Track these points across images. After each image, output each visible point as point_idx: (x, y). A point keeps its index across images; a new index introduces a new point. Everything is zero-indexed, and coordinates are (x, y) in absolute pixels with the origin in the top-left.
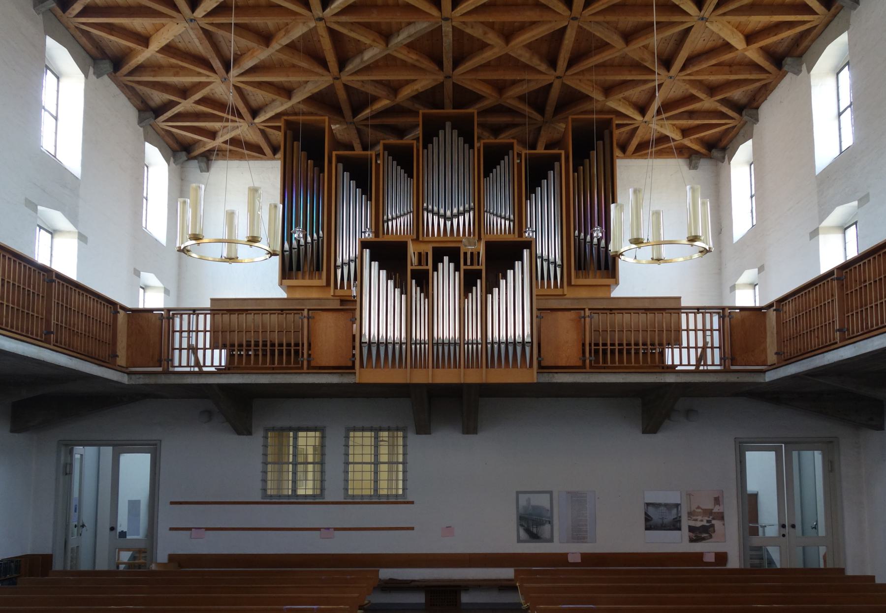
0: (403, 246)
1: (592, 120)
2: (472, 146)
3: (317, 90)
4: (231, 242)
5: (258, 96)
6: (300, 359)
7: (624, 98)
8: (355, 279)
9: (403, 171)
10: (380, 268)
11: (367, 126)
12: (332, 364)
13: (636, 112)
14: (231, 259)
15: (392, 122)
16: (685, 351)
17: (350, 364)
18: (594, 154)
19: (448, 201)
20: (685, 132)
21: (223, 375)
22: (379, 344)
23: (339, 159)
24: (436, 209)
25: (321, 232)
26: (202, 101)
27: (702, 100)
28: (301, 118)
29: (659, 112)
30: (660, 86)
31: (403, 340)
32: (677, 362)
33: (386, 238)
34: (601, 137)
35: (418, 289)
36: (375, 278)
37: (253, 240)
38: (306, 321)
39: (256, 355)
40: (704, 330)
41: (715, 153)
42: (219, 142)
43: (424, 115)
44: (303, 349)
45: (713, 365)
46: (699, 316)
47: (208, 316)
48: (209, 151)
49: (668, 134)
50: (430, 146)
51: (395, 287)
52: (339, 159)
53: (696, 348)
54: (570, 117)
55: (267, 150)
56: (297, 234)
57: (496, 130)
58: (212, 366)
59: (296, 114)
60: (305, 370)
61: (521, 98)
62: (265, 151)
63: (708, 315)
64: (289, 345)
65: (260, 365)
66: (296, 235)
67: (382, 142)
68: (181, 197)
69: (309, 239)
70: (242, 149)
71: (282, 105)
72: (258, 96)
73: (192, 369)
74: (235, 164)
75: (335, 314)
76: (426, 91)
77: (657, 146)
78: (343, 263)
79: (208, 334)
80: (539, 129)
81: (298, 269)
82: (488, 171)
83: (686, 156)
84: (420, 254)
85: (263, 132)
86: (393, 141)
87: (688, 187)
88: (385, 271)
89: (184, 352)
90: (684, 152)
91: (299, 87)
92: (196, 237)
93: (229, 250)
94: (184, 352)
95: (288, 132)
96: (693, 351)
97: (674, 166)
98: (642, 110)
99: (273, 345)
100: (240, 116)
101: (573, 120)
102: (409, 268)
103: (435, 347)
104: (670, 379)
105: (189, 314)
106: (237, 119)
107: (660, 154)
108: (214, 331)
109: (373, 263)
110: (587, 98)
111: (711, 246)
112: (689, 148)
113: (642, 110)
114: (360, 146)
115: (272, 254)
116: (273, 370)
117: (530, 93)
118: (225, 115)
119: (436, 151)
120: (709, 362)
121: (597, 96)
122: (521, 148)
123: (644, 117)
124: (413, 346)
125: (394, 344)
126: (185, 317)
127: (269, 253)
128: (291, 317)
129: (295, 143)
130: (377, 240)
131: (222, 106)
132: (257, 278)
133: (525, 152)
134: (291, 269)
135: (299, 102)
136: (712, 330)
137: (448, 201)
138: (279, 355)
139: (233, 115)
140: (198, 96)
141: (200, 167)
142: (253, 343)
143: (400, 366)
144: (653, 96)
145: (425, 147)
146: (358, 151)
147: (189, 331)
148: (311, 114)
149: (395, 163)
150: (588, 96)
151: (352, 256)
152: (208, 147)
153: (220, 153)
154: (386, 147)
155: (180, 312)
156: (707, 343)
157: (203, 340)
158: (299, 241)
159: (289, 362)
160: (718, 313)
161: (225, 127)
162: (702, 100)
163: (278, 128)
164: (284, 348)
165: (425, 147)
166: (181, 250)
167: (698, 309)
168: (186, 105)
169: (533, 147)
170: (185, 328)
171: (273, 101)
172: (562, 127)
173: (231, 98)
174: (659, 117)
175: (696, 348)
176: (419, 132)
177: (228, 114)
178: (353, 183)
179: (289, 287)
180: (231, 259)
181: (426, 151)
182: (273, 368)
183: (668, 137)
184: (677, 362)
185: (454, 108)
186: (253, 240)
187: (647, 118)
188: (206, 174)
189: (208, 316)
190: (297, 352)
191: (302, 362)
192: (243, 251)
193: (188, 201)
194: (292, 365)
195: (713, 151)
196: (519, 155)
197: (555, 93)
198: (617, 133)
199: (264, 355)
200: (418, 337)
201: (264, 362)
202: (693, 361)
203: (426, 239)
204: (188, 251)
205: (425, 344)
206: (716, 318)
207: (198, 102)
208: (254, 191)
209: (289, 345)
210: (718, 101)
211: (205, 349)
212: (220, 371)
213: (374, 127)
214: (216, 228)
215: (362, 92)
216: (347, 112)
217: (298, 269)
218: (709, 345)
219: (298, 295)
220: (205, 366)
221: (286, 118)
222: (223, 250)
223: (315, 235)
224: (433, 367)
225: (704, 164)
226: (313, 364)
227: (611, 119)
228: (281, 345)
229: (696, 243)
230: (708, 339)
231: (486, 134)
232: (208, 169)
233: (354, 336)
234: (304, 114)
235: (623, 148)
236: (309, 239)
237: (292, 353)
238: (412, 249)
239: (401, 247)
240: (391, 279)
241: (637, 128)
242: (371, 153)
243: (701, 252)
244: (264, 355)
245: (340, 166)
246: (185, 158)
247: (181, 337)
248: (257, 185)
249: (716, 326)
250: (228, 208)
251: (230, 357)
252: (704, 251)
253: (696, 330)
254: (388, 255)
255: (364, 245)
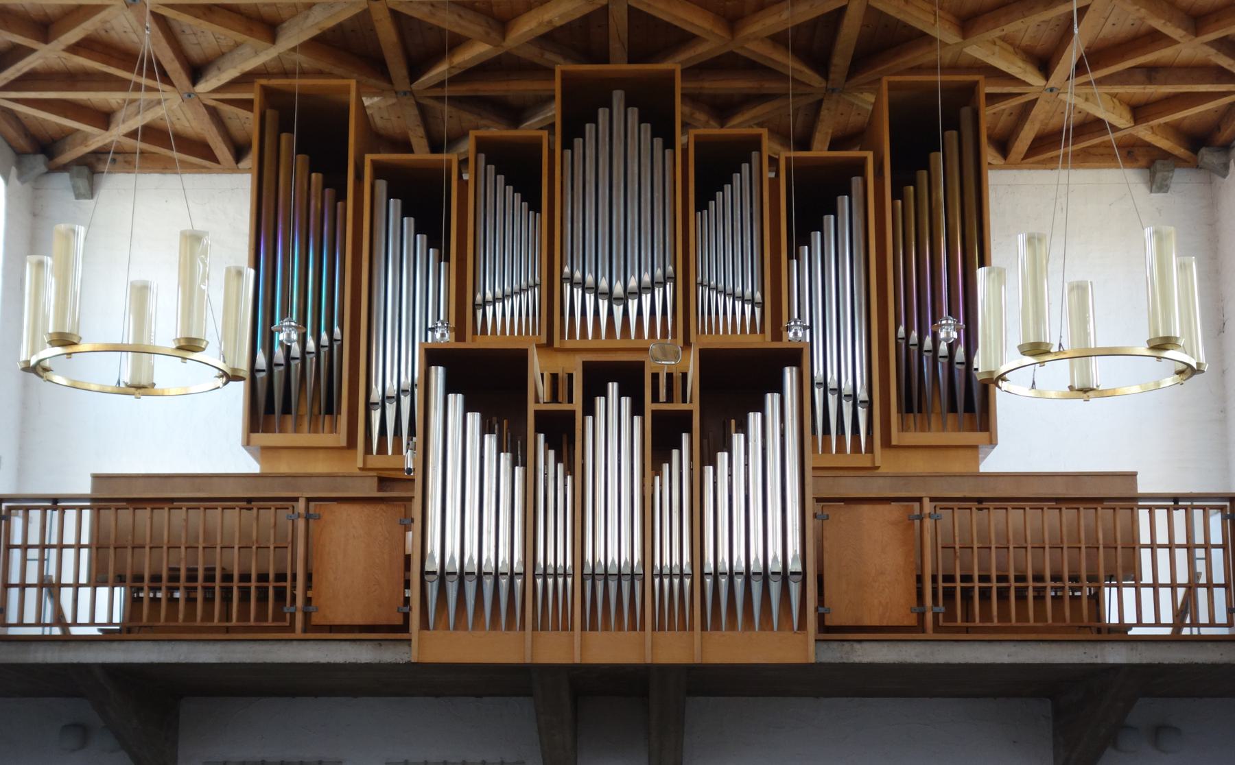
0: (518, 360)
1: (931, 89)
2: (669, 143)
3: (331, 23)
4: (139, 350)
5: (204, 36)
6: (288, 608)
7: (1004, 39)
8: (412, 432)
9: (518, 196)
10: (468, 407)
11: (440, 99)
12: (359, 620)
13: (1029, 68)
14: (140, 388)
15: (493, 92)
16: (1147, 593)
17: (398, 621)
18: (937, 158)
19: (618, 262)
20: (1139, 111)
21: (115, 645)
22: (462, 576)
23: (380, 171)
24: (590, 279)
25: (337, 330)
26: (84, 46)
27: (1174, 42)
28: (297, 83)
29: (1080, 69)
30: (1082, 11)
31: (518, 568)
32: (1130, 618)
33: (481, 343)
34: (953, 123)
35: (552, 453)
36: (457, 429)
37: (189, 346)
38: (301, 524)
39: (191, 601)
40: (1190, 547)
41: (1208, 156)
42: (116, 134)
43: (565, 75)
44: (294, 587)
45: (1212, 624)
46: (1179, 515)
47: (86, 514)
48: (96, 153)
49: (1101, 114)
50: (578, 142)
51: (500, 450)
52: (380, 171)
53: (1173, 586)
54: (885, 80)
55: (222, 151)
56: (286, 334)
57: (723, 109)
58: (92, 623)
59: (286, 74)
60: (299, 633)
61: (778, 39)
62: (218, 153)
63: (1198, 514)
64: (263, 577)
65: (252, 623)
66: (282, 337)
67: (473, 134)
68: (32, 252)
69: (311, 345)
70: (166, 148)
71: (255, 56)
72: (204, 36)
73: (47, 631)
74: (151, 182)
75: (367, 510)
76: (570, 24)
77: (1078, 142)
78: (385, 398)
79: (85, 553)
80: (819, 103)
81: (286, 409)
82: (706, 192)
83: (1143, 162)
84: (554, 377)
85: (213, 113)
86: (496, 131)
87: (1148, 231)
88: (477, 415)
89: (31, 593)
90: (1135, 154)
91: (293, 16)
92: (64, 340)
93: (136, 369)
94: (31, 593)
95: (269, 112)
96: (1165, 594)
97: (1121, 182)
98: (1045, 64)
99: (227, 577)
100: (166, 78)
101: (892, 87)
102: (532, 407)
103: (588, 583)
104: (1115, 655)
105: (45, 509)
106: (158, 84)
107: (1084, 158)
108: (98, 546)
109: (451, 397)
110: (922, 38)
111: (1203, 360)
112: (1149, 146)
113: (1045, 64)
114: (424, 142)
115: (230, 377)
116: (227, 633)
117: (797, 28)
118: (133, 77)
119: (590, 153)
120: (1204, 618)
121: (945, 33)
122: (777, 147)
123: (1047, 78)
124: (539, 581)
125: (497, 575)
126: (35, 515)
127: (224, 374)
128: (268, 516)
129: (284, 136)
130: (461, 345)
131: (126, 56)
132: (196, 430)
133: (786, 154)
134: (270, 409)
135: (294, 49)
136: (1207, 546)
137: (618, 262)
138: (259, 600)
139: (151, 75)
140: (74, 36)
141: (75, 188)
142: (183, 573)
143: (510, 626)
144: (1066, 35)
145: (567, 144)
146: (421, 154)
147: (43, 547)
148: (320, 73)
149: (501, 178)
150: (923, 35)
151: (406, 381)
152: (94, 145)
153: (119, 158)
154: (483, 146)
155: (24, 503)
156: (1198, 575)
157: (73, 566)
158: (288, 349)
159: (262, 615)
160: (1222, 509)
161: (132, 101)
162: (1174, 42)
163: (246, 104)
164: (253, 584)
165: (567, 144)
166: (30, 369)
167: (1176, 499)
168: (48, 55)
169: (804, 143)
170: (34, 539)
171: (238, 45)
172: (868, 102)
173: (147, 41)
174: (1082, 79)
175: (1173, 586)
176: (554, 112)
177: (140, 74)
178: (409, 223)
179: (265, 449)
180: (139, 387)
181: (568, 153)
182: (228, 630)
183: (1100, 121)
184: (1130, 618)
185: (629, 62)
186: (189, 346)
187: (1054, 81)
188: (87, 203)
189: (86, 514)
190: (280, 594)
191: (293, 615)
192: (166, 371)
193: (49, 261)
194: (270, 623)
195: (1203, 151)
196: (774, 162)
197: (850, 29)
198: (988, 114)
199: (209, 600)
200: (551, 560)
201: (208, 615)
202: (1167, 616)
203: (569, 344)
204: (46, 370)
205: (565, 575)
206: (1216, 520)
207: (75, 49)
208: (193, 239)
209: (263, 577)
210: (1212, 44)
211: (76, 586)
212: (109, 636)
213: (456, 101)
214: (107, 320)
215: (432, 28)
216: (398, 69)
217: (286, 409)
218: (1203, 580)
219: (284, 466)
220: (75, 623)
221: (264, 82)
222: (122, 368)
223: (324, 337)
224: (583, 628)
225: (1182, 180)
226: (316, 620)
227: (976, 83)
228: (245, 577)
229: (1167, 354)
230: (1201, 566)
231: (701, 117)
232: (91, 192)
233: (408, 559)
234: (304, 73)
235: (1003, 146)
236: (311, 345)
237: (270, 595)
238: (538, 368)
239: (518, 360)
240: (491, 432)
241: (1033, 102)
242: (449, 158)
243: (1180, 373)
244: (209, 600)
245: (382, 185)
246: (43, 169)
247: (24, 560)
248: (199, 226)
249: (1216, 537)
250: (136, 276)
251: (133, 603)
252: (1187, 371)
253: (1171, 546)
254: (485, 379)
255: (433, 356)
